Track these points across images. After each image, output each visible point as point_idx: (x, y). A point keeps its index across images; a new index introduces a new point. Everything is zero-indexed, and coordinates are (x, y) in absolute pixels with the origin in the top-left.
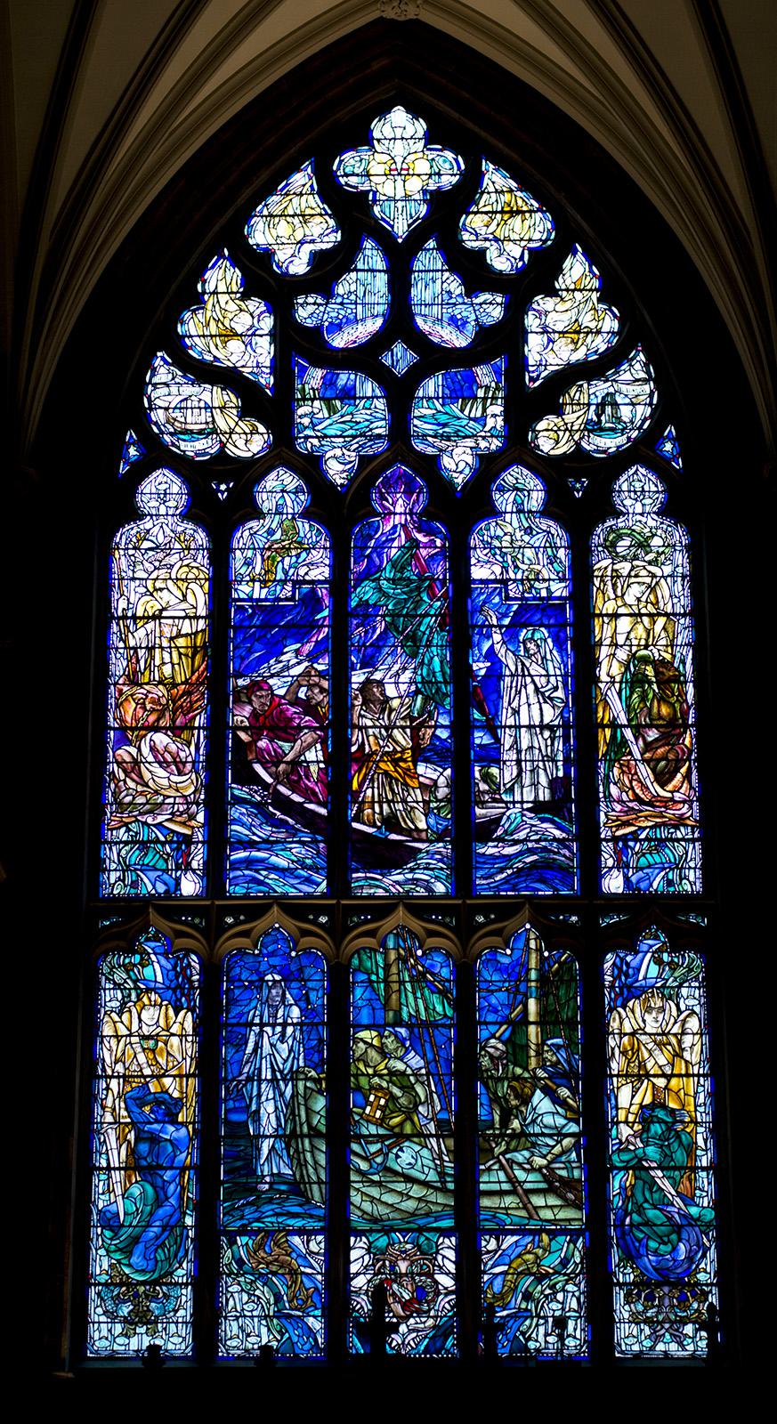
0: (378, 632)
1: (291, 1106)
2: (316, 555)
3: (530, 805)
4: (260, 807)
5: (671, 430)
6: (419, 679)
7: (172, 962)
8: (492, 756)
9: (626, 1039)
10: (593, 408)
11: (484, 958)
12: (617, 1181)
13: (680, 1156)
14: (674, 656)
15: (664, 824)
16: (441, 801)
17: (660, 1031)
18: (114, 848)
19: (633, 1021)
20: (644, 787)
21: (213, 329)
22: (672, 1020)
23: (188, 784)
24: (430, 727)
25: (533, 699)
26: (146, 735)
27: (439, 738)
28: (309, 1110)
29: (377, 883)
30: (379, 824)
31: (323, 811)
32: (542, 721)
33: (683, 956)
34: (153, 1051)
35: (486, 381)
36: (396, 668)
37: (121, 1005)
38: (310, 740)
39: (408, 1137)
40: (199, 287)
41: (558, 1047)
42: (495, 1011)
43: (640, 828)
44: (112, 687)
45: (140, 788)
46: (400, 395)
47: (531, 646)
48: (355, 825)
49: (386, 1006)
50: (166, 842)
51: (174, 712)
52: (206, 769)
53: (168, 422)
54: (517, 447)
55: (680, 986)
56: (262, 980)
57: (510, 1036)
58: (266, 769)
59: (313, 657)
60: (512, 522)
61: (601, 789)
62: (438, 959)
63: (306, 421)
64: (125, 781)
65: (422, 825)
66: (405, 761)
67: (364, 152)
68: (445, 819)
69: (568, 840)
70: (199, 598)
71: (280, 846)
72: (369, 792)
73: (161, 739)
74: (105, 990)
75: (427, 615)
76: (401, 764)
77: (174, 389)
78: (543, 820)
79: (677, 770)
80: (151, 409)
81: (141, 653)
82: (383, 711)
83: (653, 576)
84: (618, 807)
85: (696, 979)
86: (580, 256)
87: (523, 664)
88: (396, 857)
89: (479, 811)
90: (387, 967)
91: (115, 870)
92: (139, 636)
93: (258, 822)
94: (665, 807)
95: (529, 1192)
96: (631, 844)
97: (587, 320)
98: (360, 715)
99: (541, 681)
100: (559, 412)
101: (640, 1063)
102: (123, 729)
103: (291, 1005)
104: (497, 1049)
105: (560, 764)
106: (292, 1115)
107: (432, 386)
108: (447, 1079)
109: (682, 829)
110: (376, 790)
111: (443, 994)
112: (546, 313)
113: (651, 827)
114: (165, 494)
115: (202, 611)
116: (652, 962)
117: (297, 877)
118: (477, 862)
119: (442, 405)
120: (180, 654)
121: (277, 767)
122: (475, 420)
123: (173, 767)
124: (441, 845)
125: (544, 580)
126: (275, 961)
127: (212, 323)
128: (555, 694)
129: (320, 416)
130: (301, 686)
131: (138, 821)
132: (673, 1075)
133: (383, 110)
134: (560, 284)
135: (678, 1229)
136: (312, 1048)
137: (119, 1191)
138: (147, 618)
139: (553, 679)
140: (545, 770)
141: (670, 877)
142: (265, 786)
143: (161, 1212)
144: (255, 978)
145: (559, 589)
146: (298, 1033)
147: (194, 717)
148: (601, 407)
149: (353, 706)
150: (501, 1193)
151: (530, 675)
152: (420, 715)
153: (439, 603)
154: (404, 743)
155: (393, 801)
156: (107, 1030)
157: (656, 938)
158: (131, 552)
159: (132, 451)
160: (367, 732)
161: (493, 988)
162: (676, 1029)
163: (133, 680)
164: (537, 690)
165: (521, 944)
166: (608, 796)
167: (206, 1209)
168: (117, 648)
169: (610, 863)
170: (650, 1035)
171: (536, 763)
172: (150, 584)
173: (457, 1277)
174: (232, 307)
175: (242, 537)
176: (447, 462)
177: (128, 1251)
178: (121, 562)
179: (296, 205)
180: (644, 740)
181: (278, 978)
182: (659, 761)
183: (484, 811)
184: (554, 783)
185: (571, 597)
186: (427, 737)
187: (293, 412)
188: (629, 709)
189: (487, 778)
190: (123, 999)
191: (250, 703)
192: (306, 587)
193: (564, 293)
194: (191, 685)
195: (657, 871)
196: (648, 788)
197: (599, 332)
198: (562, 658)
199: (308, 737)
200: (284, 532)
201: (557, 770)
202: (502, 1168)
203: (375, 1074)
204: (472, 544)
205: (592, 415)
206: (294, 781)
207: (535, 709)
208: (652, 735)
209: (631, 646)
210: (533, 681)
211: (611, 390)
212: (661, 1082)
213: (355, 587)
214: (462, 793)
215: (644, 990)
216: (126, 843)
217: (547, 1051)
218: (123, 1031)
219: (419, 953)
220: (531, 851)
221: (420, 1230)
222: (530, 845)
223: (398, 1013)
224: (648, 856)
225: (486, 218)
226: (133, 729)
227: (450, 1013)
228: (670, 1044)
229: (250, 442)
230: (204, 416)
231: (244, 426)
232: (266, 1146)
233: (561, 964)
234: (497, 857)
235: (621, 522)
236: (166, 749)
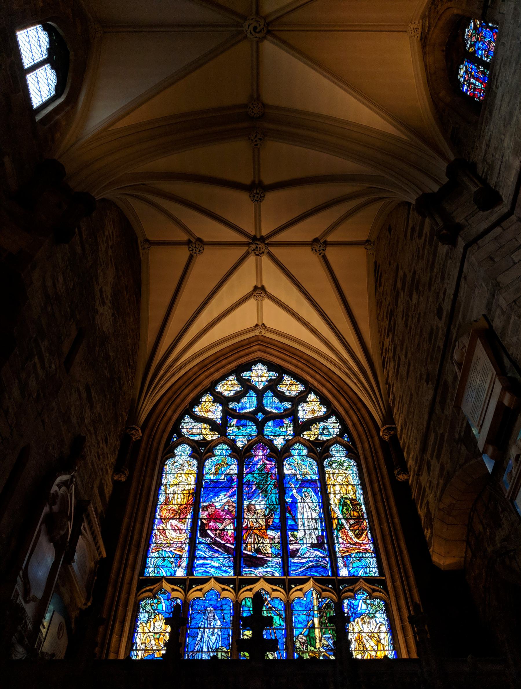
0: (253, 489)
2: (233, 467)
3: (310, 545)
6: (268, 503)
7: (170, 602)
8: (294, 528)
9: (356, 635)
10: (321, 429)
11: (295, 601)
14: (356, 497)
15: (360, 552)
16: (276, 543)
17: (370, 631)
18: (152, 559)
19: (358, 627)
20: (351, 539)
21: (204, 410)
22: (374, 627)
23: (184, 537)
24: (272, 519)
25: (308, 510)
26: (169, 521)
27: (275, 522)
29: (252, 572)
30: (253, 551)
31: (232, 547)
32: (312, 517)
33: (375, 601)
34: (158, 639)
35: (287, 422)
36: (260, 500)
37: (147, 620)
38: (228, 523)
40: (200, 400)
41: (328, 638)
42: (301, 623)
43: (352, 553)
44: (159, 506)
45: (165, 538)
46: (260, 426)
47: (306, 494)
48: (244, 552)
50: (173, 557)
51: (180, 514)
52: (190, 532)
53: (187, 432)
55: (376, 613)
56: (206, 610)
57: (308, 634)
58: (212, 532)
59: (230, 496)
60: (297, 458)
61: (335, 539)
62: (277, 601)
63: (231, 432)
64: (159, 536)
65: (270, 552)
66: (263, 530)
68: (278, 549)
69: (325, 557)
70: (193, 479)
71: (216, 559)
72: (250, 540)
73: (174, 522)
74: (141, 613)
75: (270, 484)
76: (262, 531)
77: (190, 424)
78: (315, 550)
79: (363, 533)
80: (182, 428)
81: (171, 496)
82: (255, 513)
83: (346, 474)
84: (342, 546)
85: (381, 610)
86: (313, 394)
87: (304, 499)
89: (291, 547)
91: (152, 567)
92: (170, 490)
93: (208, 550)
94: (360, 546)
96: (349, 558)
97: (316, 408)
98: (247, 515)
99: (310, 504)
100: (310, 430)
101: (363, 645)
103: (217, 620)
104: (302, 639)
105: (320, 531)
108: (282, 652)
109: (368, 553)
110: (252, 540)
112: (304, 407)
113: (356, 553)
114: (184, 450)
115: (193, 483)
116: (363, 604)
117: (222, 570)
118: (291, 565)
119: (274, 428)
120: (184, 496)
121: (216, 532)
122: (284, 432)
123: (178, 531)
124: (277, 558)
125: (309, 474)
126: (212, 602)
127: (203, 408)
128: (316, 509)
129: (235, 430)
130: (225, 505)
131: (162, 550)
132: (378, 650)
134: (308, 400)
136: (225, 638)
138: (174, 485)
139: (315, 504)
140: (314, 533)
141: (366, 571)
142: (212, 538)
144: (203, 609)
145: (315, 477)
146: (219, 632)
147: (187, 515)
149: (244, 512)
151: (306, 502)
152: (268, 515)
153: (274, 481)
154: (262, 523)
155: (259, 543)
156: (140, 630)
157: (363, 594)
158: (171, 466)
160: (249, 519)
161: (299, 613)
162: (376, 631)
163: (166, 503)
164: (309, 507)
165: (310, 596)
166: (339, 543)
168: (162, 494)
169: (342, 565)
170: (366, 633)
171: (311, 531)
172: (176, 475)
174: (210, 405)
175: (208, 462)
176: (275, 442)
178: (167, 469)
180: (350, 523)
181: (212, 609)
182: (356, 530)
183: (293, 547)
184: (317, 537)
185: (319, 479)
186: (271, 522)
187: (226, 430)
188: (343, 513)
189: (293, 535)
190: (148, 617)
191: (207, 510)
192: (229, 476)
193: (309, 402)
194: (187, 505)
195: (360, 568)
196: (352, 539)
197: (320, 411)
198: (317, 497)
199: (227, 521)
200: (223, 461)
201: (319, 532)
204: (284, 464)
205: (321, 431)
206: (222, 537)
208: (352, 522)
209: (341, 494)
210: (308, 505)
211: (326, 425)
213: (245, 476)
214: (284, 542)
215: (361, 614)
216: (157, 558)
217: (324, 640)
219: (269, 599)
220: (311, 561)
222: (311, 559)
224: (356, 563)
225: (285, 386)
226: (164, 519)
227: (282, 623)
228: (375, 637)
229: (212, 436)
230: (199, 430)
231: (211, 433)
233: (326, 604)
234: (299, 563)
235: (333, 459)
236: (176, 525)
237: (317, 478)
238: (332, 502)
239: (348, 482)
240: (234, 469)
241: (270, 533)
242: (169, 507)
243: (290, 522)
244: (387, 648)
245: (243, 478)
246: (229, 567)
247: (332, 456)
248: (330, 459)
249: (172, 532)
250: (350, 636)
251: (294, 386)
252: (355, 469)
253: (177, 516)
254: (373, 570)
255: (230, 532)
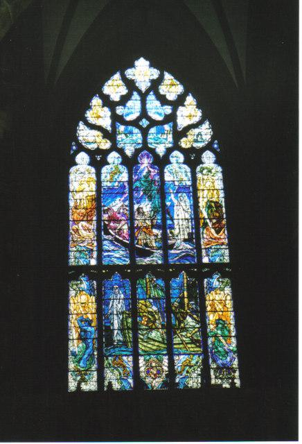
1: (122, 321)
4: (111, 241)
5: (216, 141)
8: (172, 227)
12: (210, 340)
13: (226, 333)
23: (92, 235)
25: (183, 212)
28: (127, 322)
39: (154, 329)
46: (145, 132)
47: (182, 198)
49: (147, 294)
54: (176, 147)
59: (124, 201)
63: (120, 140)
67: (133, 69)
70: (93, 186)
73: (84, 223)
81: (78, 201)
88: (148, 254)
89: (169, 242)
90: (146, 283)
92: (78, 196)
95: (187, 343)
97: (193, 113)
99: (184, 207)
100: (186, 136)
102: (74, 221)
106: (122, 324)
107: (153, 130)
111: (162, 290)
115: (94, 189)
133: (137, 58)
134: (186, 103)
135: (227, 353)
137: (76, 345)
142: (112, 236)
143: (88, 351)
145: (189, 183)
148: (198, 135)
150: (179, 344)
156: (71, 301)
159: (74, 148)
160: (139, 222)
163: (76, 208)
166: (203, 238)
167: (100, 349)
169: (204, 255)
173: (168, 367)
175: (105, 170)
177: (79, 362)
178: (72, 177)
179: (115, 83)
184: (189, 234)
185: (192, 185)
188: (208, 214)
189: (171, 233)
199: (123, 222)
202: (179, 337)
203: (145, 312)
207: (183, 214)
208: (214, 221)
212: (221, 313)
214: (165, 237)
215: (215, 288)
218: (76, 302)
220: (183, 252)
221: (158, 354)
223: (150, 295)
229: (106, 145)
230: (93, 138)
231: (104, 141)
232: (116, 332)
235: (204, 166)
237: (190, 184)
238: (200, 205)
239: (214, 187)
240: (124, 177)
241: (155, 231)
242: (78, 211)
243: (169, 222)
244: (229, 310)
245: (133, 185)
246: (127, 257)
247: (203, 163)
248: (201, 165)
249: (83, 231)
250: (207, 303)
251: (173, 87)
252: (220, 175)
253: (85, 219)
254: (226, 258)
255: (125, 231)
